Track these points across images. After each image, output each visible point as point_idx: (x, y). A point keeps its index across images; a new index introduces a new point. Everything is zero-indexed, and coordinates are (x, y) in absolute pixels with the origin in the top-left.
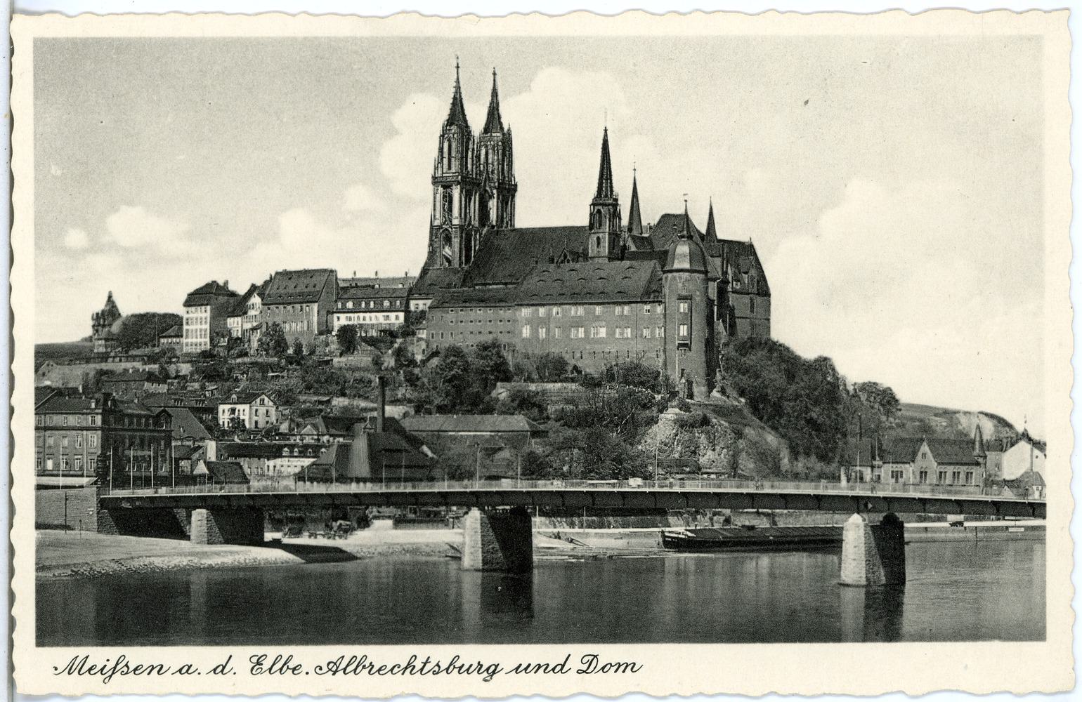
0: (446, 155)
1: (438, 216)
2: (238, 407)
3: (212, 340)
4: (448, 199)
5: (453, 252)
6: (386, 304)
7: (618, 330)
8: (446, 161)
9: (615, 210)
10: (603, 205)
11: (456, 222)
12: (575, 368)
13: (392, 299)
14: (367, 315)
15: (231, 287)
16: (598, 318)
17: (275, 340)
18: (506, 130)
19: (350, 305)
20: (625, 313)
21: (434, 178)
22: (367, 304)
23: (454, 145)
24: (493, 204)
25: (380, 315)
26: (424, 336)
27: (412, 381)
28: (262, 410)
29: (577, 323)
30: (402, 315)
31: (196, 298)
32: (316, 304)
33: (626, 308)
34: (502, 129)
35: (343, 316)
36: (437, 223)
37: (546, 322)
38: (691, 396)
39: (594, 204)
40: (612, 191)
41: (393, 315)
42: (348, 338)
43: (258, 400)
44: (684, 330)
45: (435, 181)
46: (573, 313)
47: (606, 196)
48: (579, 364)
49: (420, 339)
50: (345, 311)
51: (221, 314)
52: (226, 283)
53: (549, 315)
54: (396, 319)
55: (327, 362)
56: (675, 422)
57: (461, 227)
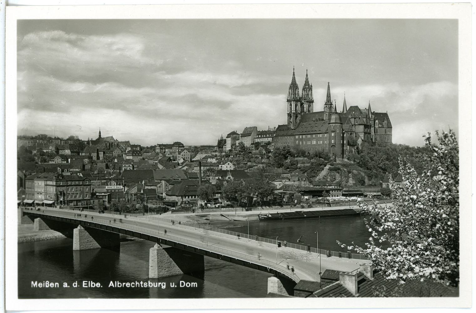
0: (290, 93)
1: (289, 110)
2: (223, 166)
3: (231, 146)
4: (291, 105)
5: (292, 120)
6: (268, 136)
7: (319, 142)
8: (290, 95)
9: (331, 106)
10: (327, 105)
11: (292, 112)
12: (308, 153)
13: (269, 134)
14: (263, 139)
15: (237, 133)
16: (314, 138)
17: (242, 147)
18: (310, 85)
19: (260, 136)
20: (321, 136)
21: (288, 100)
22: (264, 136)
23: (292, 90)
24: (306, 106)
25: (266, 139)
26: (273, 145)
27: (268, 158)
28: (229, 166)
29: (310, 140)
30: (271, 138)
31: (229, 136)
32: (250, 137)
33: (321, 135)
34: (309, 85)
35: (258, 139)
36: (288, 112)
37: (302, 139)
38: (335, 161)
39: (325, 105)
40: (330, 101)
41: (269, 139)
42: (257, 145)
43: (227, 163)
44: (333, 141)
45: (288, 101)
46: (308, 137)
47: (329, 102)
48: (310, 152)
49: (272, 145)
50: (258, 138)
51: (235, 139)
52: (236, 131)
53: (302, 137)
54: (270, 139)
55: (250, 153)
56: (328, 169)
57: (294, 113)
